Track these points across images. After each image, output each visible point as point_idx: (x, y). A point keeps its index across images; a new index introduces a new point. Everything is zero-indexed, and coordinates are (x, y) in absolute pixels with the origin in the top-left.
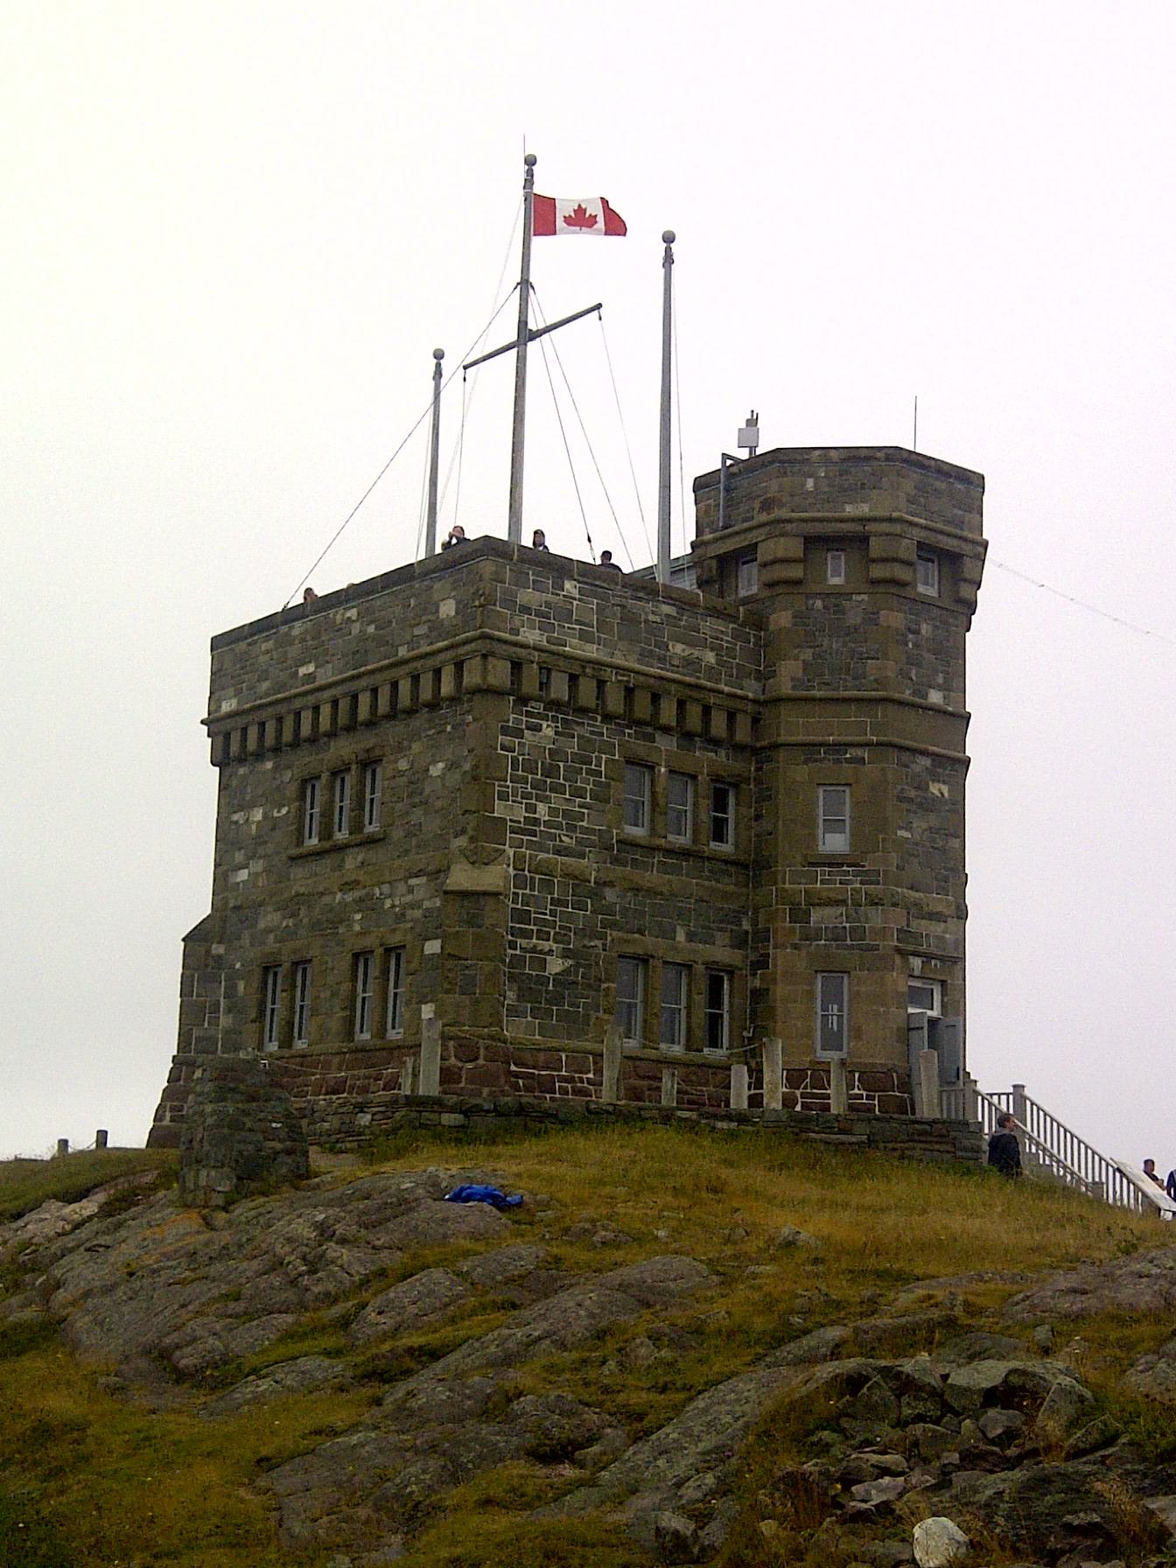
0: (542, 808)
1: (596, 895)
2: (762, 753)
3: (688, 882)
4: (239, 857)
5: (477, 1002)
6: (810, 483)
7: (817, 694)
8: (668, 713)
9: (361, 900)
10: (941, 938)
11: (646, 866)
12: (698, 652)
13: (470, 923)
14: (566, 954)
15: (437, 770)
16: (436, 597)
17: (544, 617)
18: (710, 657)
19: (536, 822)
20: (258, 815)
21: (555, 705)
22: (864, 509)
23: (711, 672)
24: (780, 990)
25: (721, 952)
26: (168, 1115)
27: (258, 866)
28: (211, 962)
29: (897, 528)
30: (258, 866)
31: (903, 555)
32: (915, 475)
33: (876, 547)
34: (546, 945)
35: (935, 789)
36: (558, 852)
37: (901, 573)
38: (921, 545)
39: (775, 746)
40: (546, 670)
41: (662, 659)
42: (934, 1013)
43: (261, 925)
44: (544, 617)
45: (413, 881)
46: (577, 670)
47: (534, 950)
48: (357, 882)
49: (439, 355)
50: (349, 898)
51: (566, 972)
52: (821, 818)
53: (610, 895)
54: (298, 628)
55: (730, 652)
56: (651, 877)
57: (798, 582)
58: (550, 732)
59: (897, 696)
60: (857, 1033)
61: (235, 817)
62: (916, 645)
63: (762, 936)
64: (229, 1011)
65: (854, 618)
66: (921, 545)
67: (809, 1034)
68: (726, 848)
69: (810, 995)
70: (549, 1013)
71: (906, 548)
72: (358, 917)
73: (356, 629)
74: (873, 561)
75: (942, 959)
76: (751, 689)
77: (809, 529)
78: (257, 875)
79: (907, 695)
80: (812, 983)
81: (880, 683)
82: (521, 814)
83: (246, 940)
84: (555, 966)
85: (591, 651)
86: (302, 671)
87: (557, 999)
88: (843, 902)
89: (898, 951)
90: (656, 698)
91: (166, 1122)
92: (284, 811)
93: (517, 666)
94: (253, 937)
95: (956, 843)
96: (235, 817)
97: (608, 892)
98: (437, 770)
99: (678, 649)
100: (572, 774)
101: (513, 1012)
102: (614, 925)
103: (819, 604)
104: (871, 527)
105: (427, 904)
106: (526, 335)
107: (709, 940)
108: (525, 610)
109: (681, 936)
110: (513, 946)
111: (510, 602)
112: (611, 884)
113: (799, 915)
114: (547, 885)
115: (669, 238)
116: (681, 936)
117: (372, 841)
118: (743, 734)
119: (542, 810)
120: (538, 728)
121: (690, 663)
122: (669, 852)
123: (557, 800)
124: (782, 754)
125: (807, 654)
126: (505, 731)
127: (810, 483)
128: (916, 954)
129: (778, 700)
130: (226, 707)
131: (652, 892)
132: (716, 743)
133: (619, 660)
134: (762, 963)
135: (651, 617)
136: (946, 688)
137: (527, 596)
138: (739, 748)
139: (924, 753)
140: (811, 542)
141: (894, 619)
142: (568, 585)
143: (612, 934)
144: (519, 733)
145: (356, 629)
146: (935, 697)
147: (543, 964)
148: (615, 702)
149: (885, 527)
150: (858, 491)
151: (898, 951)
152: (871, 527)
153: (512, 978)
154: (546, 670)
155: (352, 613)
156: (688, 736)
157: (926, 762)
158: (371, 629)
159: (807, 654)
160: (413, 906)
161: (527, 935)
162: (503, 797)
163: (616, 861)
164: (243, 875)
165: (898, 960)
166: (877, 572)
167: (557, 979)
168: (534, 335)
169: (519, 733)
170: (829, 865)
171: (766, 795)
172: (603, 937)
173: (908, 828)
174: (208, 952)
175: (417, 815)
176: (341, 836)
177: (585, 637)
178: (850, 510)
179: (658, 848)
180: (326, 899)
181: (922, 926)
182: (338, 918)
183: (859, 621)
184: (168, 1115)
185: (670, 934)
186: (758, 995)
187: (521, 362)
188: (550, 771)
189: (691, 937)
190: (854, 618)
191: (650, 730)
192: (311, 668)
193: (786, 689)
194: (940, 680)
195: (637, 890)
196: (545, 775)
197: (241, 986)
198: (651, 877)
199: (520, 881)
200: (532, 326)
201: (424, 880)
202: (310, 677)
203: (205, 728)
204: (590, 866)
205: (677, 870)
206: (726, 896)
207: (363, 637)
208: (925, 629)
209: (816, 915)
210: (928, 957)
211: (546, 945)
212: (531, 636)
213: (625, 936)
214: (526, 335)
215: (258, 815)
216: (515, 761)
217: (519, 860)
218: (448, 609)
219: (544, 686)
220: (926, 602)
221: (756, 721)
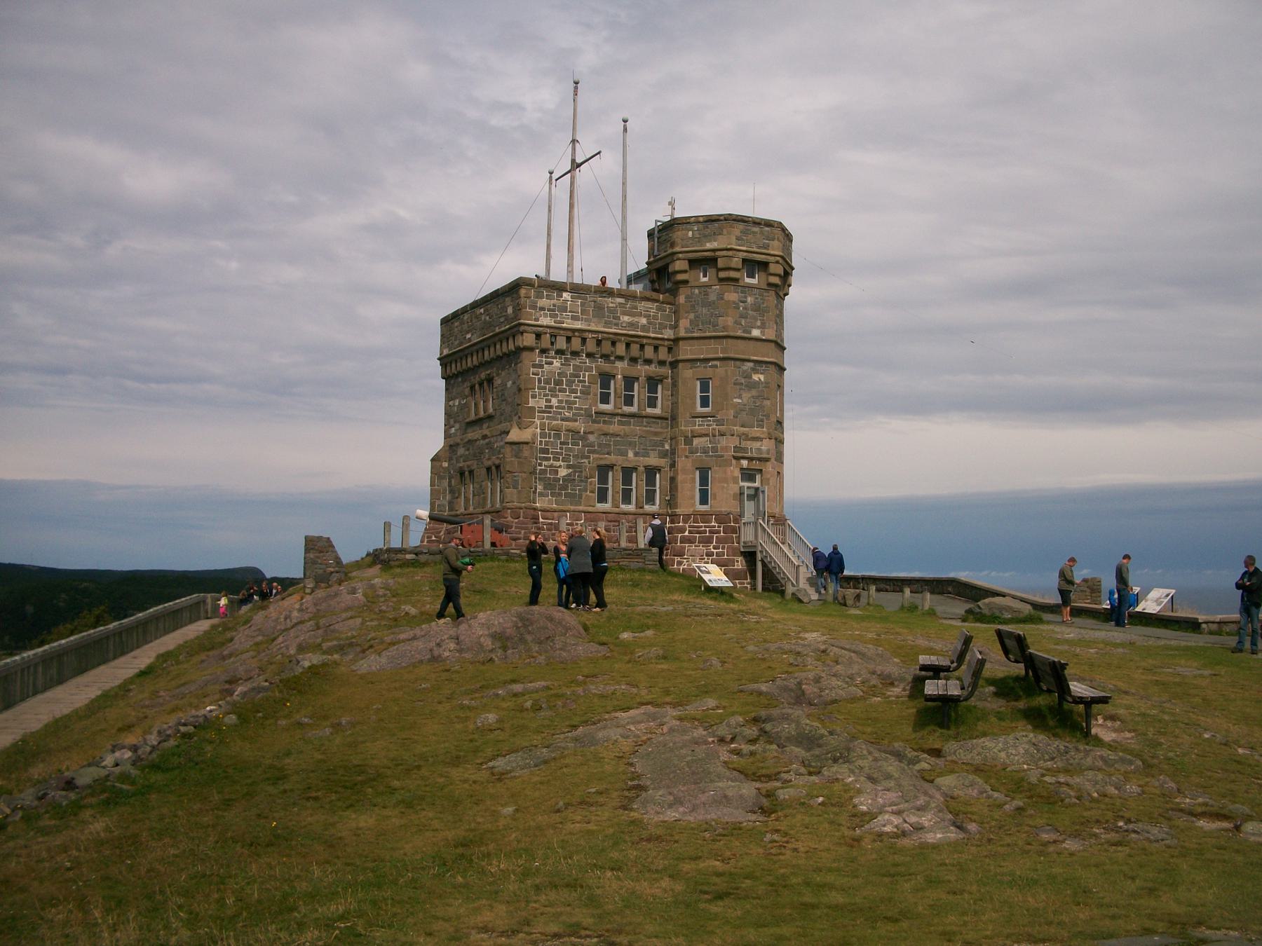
0: (554, 401)
1: (584, 438)
2: (674, 365)
3: (636, 428)
7: (695, 335)
8: (621, 349)
10: (759, 450)
11: (610, 423)
12: (643, 318)
13: (516, 456)
14: (568, 467)
15: (509, 384)
18: (644, 321)
19: (551, 407)
21: (560, 352)
22: (714, 245)
23: (644, 328)
24: (680, 478)
25: (653, 460)
27: (457, 426)
29: (730, 253)
30: (457, 426)
31: (733, 265)
32: (741, 226)
33: (721, 263)
34: (558, 464)
35: (755, 377)
37: (733, 274)
38: (744, 261)
39: (677, 362)
40: (554, 336)
41: (616, 325)
42: (757, 484)
44: (552, 312)
46: (570, 334)
49: (551, 173)
51: (569, 475)
52: (699, 394)
53: (592, 438)
54: (466, 317)
55: (655, 317)
56: (614, 428)
57: (686, 282)
58: (558, 365)
59: (732, 334)
62: (745, 308)
63: (673, 452)
65: (712, 297)
66: (744, 261)
67: (693, 497)
68: (657, 411)
69: (694, 479)
70: (560, 495)
71: (736, 262)
74: (719, 270)
75: (760, 459)
76: (668, 334)
79: (739, 333)
81: (725, 328)
82: (543, 403)
84: (563, 472)
86: (468, 336)
87: (565, 488)
88: (707, 435)
89: (735, 458)
90: (614, 343)
93: (538, 336)
95: (767, 403)
98: (509, 384)
99: (626, 318)
100: (570, 383)
101: (541, 495)
102: (594, 452)
103: (697, 291)
104: (718, 253)
106: (576, 165)
107: (646, 455)
108: (542, 309)
109: (631, 454)
110: (540, 465)
111: (534, 307)
112: (592, 433)
113: (688, 441)
114: (558, 436)
115: (625, 121)
116: (631, 454)
117: (490, 417)
118: (663, 354)
119: (554, 401)
120: (551, 363)
121: (631, 325)
122: (623, 415)
124: (681, 365)
125: (692, 316)
126: (534, 366)
127: (690, 234)
128: (744, 458)
129: (676, 340)
130: (446, 352)
131: (612, 435)
132: (648, 362)
134: (673, 465)
136: (762, 327)
137: (543, 302)
138: (662, 363)
139: (749, 361)
141: (732, 296)
142: (565, 295)
144: (541, 366)
146: (756, 333)
148: (591, 346)
149: (724, 253)
150: (708, 237)
151: (735, 458)
152: (718, 253)
153: (540, 479)
154: (554, 336)
156: (634, 360)
157: (751, 364)
159: (692, 316)
161: (548, 459)
162: (534, 397)
163: (594, 422)
165: (734, 462)
166: (722, 275)
167: (565, 479)
168: (579, 165)
169: (541, 366)
171: (675, 384)
173: (740, 397)
176: (482, 414)
177: (574, 318)
178: (709, 246)
179: (617, 415)
181: (749, 444)
186: (673, 479)
187: (573, 179)
188: (558, 383)
189: (636, 454)
193: (682, 334)
194: (759, 323)
195: (605, 434)
196: (556, 384)
198: (614, 428)
199: (543, 435)
200: (579, 161)
204: (581, 426)
205: (629, 424)
206: (656, 434)
208: (749, 299)
209: (696, 441)
210: (750, 459)
211: (558, 464)
212: (546, 321)
214: (576, 165)
216: (540, 381)
217: (543, 425)
218: (510, 310)
219: (552, 344)
220: (750, 287)
221: (670, 349)
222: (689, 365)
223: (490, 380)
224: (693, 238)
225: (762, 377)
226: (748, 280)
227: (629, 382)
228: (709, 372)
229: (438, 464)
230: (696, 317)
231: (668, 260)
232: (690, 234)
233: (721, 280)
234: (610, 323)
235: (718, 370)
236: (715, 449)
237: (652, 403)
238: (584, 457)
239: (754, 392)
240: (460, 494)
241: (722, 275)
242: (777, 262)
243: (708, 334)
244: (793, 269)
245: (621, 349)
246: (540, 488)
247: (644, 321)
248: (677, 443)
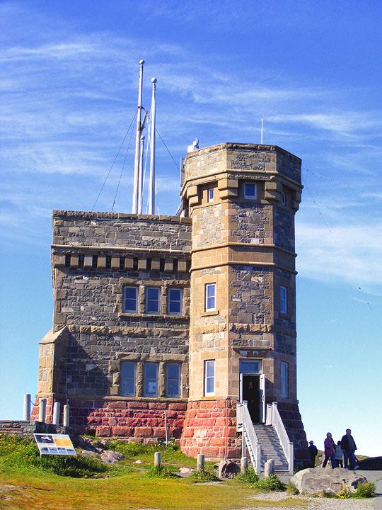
3: (158, 329)
8: (142, 264)
10: (259, 342)
17: (81, 236)
25: (173, 356)
29: (226, 175)
32: (236, 152)
34: (85, 360)
36: (89, 324)
44: (81, 236)
47: (79, 362)
53: (116, 338)
56: (138, 330)
60: (218, 386)
66: (241, 181)
70: (87, 386)
77: (198, 182)
85: (102, 246)
90: (136, 260)
93: (68, 257)
101: (70, 386)
104: (218, 177)
108: (71, 234)
116: (153, 352)
119: (82, 308)
120: (82, 278)
123: (90, 304)
125: (201, 232)
133: (117, 247)
135: (133, 228)
136: (262, 236)
137: (71, 230)
140: (201, 188)
143: (117, 353)
146: (255, 242)
147: (84, 367)
149: (221, 176)
159: (201, 232)
161: (75, 356)
167: (90, 372)
172: (114, 354)
173: (240, 296)
181: (247, 337)
189: (158, 351)
191: (136, 272)
194: (257, 233)
209: (206, 337)
213: (126, 353)
225: (261, 279)
226: (247, 197)
227: (152, 294)
230: (205, 232)
233: (223, 198)
234: (131, 243)
237: (174, 306)
238: (107, 354)
239: (253, 293)
242: (273, 180)
244: (302, 187)
245: (142, 264)
246: (68, 380)
247: (164, 239)
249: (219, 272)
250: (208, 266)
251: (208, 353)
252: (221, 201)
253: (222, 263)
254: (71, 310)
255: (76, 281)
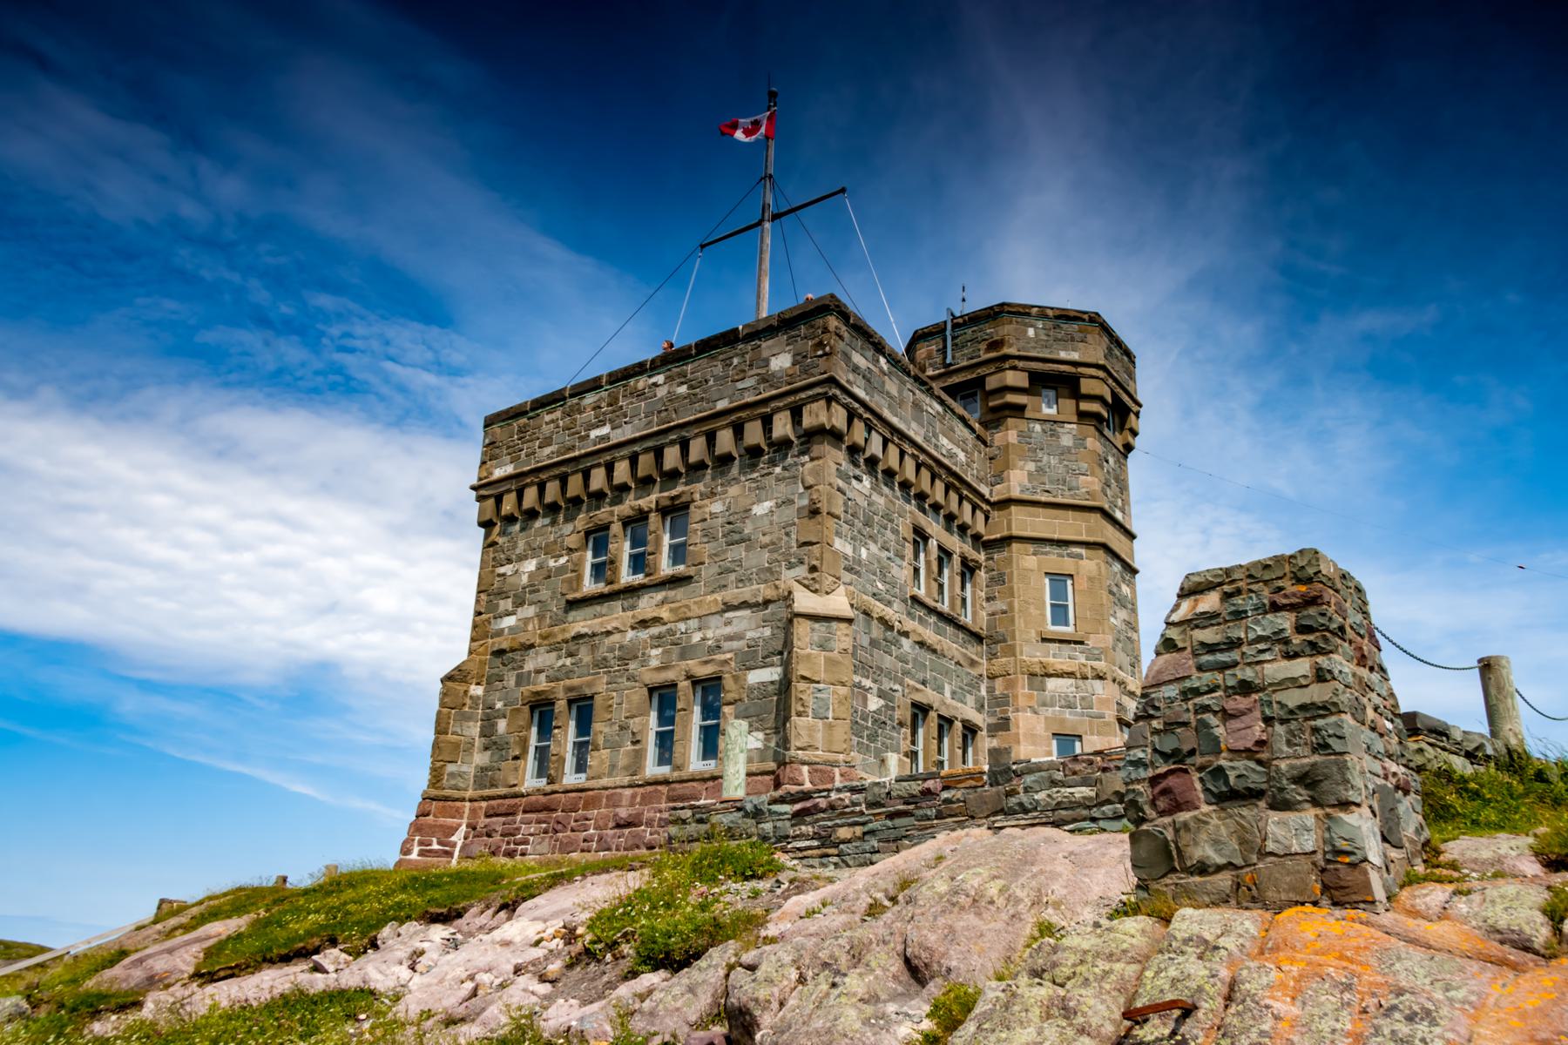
4: (506, 604)
5: (830, 726)
6: (1031, 332)
7: (1044, 498)
9: (659, 637)
13: (822, 647)
16: (765, 354)
20: (530, 566)
22: (1075, 356)
26: (416, 850)
28: (468, 701)
30: (529, 611)
33: (1087, 386)
39: (1007, 540)
43: (529, 666)
45: (727, 615)
48: (657, 620)
50: (644, 635)
52: (1048, 602)
53: (906, 644)
61: (502, 570)
64: (486, 749)
72: (654, 652)
73: (661, 392)
78: (526, 621)
80: (1050, 745)
83: (511, 681)
86: (594, 434)
88: (1071, 675)
91: (414, 856)
92: (563, 560)
94: (519, 677)
96: (502, 570)
97: (904, 640)
103: (1038, 427)
104: (1081, 370)
105: (750, 635)
109: (948, 694)
111: (847, 358)
119: (864, 553)
123: (874, 548)
125: (1031, 466)
137: (857, 359)
145: (661, 392)
149: (1092, 371)
155: (660, 379)
158: (683, 389)
159: (1031, 466)
160: (730, 638)
164: (510, 621)
166: (1084, 406)
170: (1061, 641)
174: (466, 692)
175: (739, 552)
178: (1063, 355)
180: (616, 637)
182: (628, 655)
183: (1070, 443)
184: (416, 850)
185: (939, 689)
190: (1066, 441)
192: (605, 430)
193: (1016, 493)
197: (502, 725)
201: (746, 613)
202: (605, 438)
203: (474, 493)
204: (894, 613)
207: (672, 398)
209: (1052, 684)
215: (530, 566)
222: (1031, 548)
223: (675, 511)
224: (1037, 340)
228: (1067, 565)
229: (461, 688)
230: (1040, 470)
231: (981, 371)
232: (1031, 332)
235: (1085, 562)
236: (1087, 703)
240: (525, 751)
241: (1084, 406)
243: (1060, 500)
248: (1011, 685)
249: (1080, 557)
250: (1056, 536)
251: (1062, 721)
252: (1075, 419)
253: (1084, 538)
254: (848, 550)
255: (854, 482)
